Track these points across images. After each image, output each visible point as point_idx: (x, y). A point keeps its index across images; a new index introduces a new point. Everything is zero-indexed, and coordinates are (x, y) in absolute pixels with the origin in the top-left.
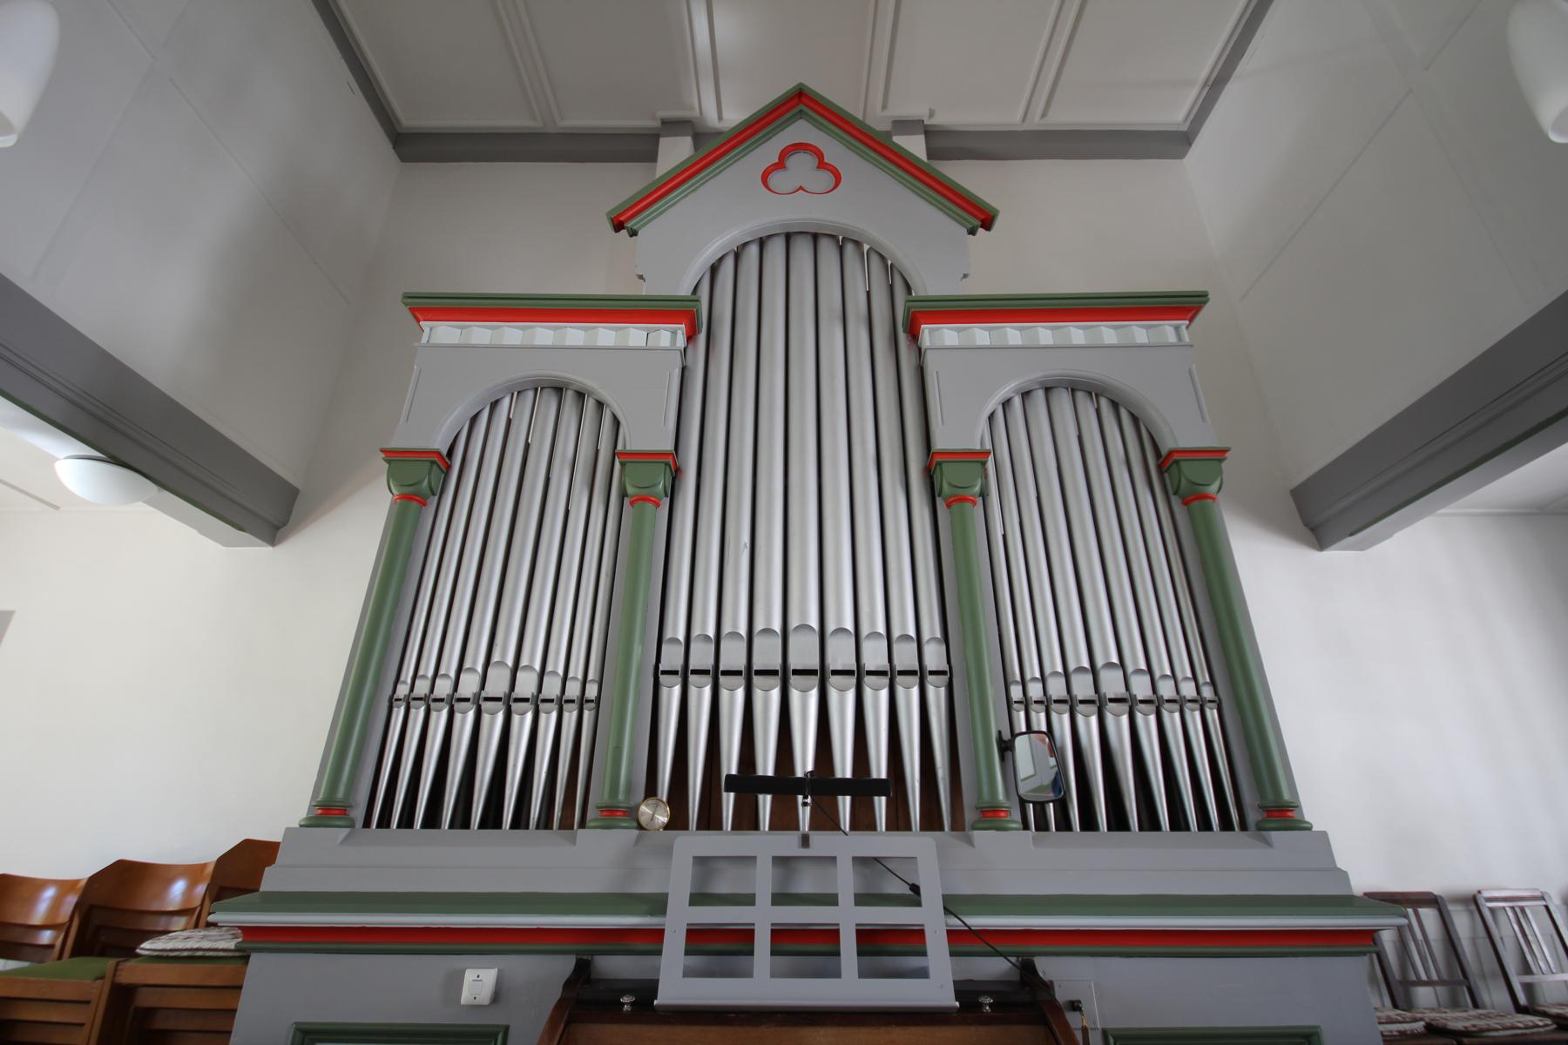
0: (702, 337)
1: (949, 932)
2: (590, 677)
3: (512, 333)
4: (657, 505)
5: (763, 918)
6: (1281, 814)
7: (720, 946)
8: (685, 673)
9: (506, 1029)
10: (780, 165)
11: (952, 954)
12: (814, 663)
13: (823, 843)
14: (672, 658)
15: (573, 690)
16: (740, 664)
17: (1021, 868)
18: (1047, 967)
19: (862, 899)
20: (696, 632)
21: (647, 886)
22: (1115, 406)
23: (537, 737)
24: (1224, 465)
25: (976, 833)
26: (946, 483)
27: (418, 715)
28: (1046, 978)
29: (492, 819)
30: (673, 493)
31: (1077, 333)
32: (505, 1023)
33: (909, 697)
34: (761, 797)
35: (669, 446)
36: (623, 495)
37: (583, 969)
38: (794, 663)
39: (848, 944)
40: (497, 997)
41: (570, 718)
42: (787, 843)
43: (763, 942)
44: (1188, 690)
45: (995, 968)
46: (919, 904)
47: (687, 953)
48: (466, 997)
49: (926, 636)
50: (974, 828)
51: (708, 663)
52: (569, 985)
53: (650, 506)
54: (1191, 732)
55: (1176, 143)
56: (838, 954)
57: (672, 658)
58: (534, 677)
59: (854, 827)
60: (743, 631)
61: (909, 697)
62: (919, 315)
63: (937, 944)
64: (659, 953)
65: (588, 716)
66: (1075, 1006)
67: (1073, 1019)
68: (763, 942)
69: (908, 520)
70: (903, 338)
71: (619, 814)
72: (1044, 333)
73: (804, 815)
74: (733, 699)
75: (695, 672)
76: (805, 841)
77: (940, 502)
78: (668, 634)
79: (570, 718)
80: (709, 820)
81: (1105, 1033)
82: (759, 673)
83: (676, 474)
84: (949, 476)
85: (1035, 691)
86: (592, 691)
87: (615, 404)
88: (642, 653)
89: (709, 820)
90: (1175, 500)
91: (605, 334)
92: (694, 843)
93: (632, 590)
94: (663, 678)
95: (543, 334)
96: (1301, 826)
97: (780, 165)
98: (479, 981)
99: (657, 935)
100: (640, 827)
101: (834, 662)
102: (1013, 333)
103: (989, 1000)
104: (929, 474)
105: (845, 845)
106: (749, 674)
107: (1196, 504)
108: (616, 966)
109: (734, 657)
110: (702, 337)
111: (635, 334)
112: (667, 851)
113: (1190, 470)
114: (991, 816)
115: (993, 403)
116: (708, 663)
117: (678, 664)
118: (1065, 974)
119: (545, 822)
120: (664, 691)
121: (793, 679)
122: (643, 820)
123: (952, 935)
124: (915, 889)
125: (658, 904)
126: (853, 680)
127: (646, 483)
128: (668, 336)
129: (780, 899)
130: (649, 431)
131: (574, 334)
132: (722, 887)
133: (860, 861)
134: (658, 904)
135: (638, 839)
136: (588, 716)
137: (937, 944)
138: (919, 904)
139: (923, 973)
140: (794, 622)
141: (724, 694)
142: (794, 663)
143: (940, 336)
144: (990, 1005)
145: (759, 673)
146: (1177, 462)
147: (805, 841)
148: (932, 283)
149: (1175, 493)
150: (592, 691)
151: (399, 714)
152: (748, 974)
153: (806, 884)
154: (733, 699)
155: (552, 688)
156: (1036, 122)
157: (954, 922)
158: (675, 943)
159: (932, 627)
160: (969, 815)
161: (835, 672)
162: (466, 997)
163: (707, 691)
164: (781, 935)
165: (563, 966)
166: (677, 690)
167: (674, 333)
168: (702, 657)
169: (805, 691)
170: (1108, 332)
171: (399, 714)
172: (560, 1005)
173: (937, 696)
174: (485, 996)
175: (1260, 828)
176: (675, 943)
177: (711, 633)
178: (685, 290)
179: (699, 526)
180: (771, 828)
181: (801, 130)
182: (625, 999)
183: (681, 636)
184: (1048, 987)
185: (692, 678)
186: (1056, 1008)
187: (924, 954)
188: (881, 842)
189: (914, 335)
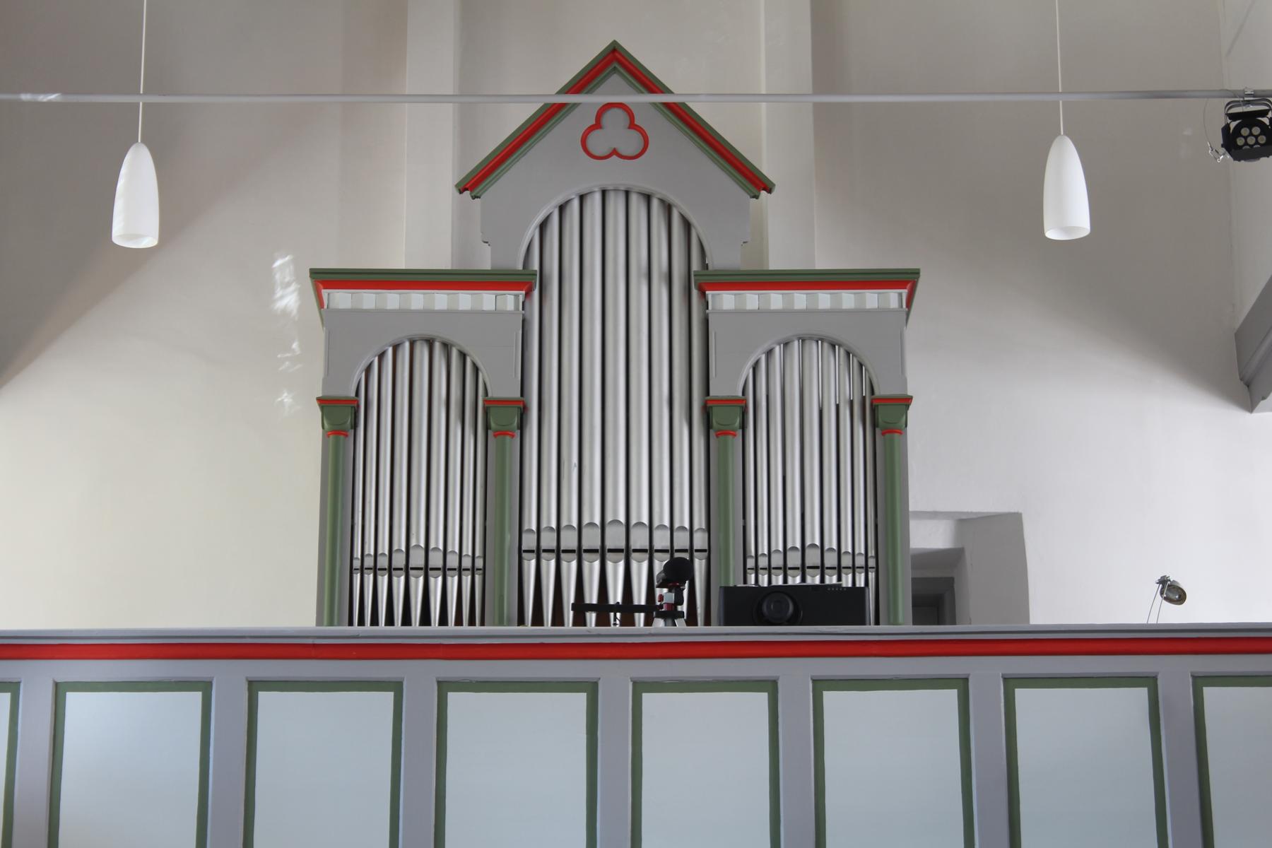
0: (536, 293)
2: (477, 554)
4: (513, 436)
10: (598, 125)
12: (622, 545)
14: (529, 542)
15: (467, 563)
16: (574, 545)
20: (544, 525)
27: (369, 578)
30: (522, 426)
34: (588, 614)
35: (517, 394)
36: (487, 427)
38: (609, 545)
41: (467, 580)
49: (696, 527)
51: (553, 545)
53: (508, 438)
57: (529, 542)
58: (441, 555)
60: (575, 524)
62: (704, 281)
65: (478, 578)
69: (688, 445)
70: (695, 293)
75: (545, 551)
77: (712, 433)
78: (526, 527)
79: (467, 580)
82: (587, 551)
84: (718, 417)
85: (763, 562)
86: (479, 563)
88: (511, 538)
94: (524, 555)
95: (417, 299)
97: (598, 125)
101: (635, 544)
109: (569, 541)
110: (536, 293)
111: (488, 300)
116: (553, 545)
117: (533, 546)
120: (525, 563)
121: (608, 555)
126: (647, 555)
127: (503, 422)
136: (478, 578)
140: (609, 518)
141: (564, 564)
142: (609, 545)
145: (587, 551)
150: (479, 563)
151: (357, 577)
155: (453, 561)
159: (700, 522)
161: (635, 551)
163: (553, 563)
166: (533, 562)
167: (516, 296)
168: (548, 541)
169: (616, 562)
170: (848, 299)
171: (357, 577)
177: (554, 525)
179: (541, 447)
181: (615, 90)
183: (534, 527)
185: (544, 555)
189: (703, 295)
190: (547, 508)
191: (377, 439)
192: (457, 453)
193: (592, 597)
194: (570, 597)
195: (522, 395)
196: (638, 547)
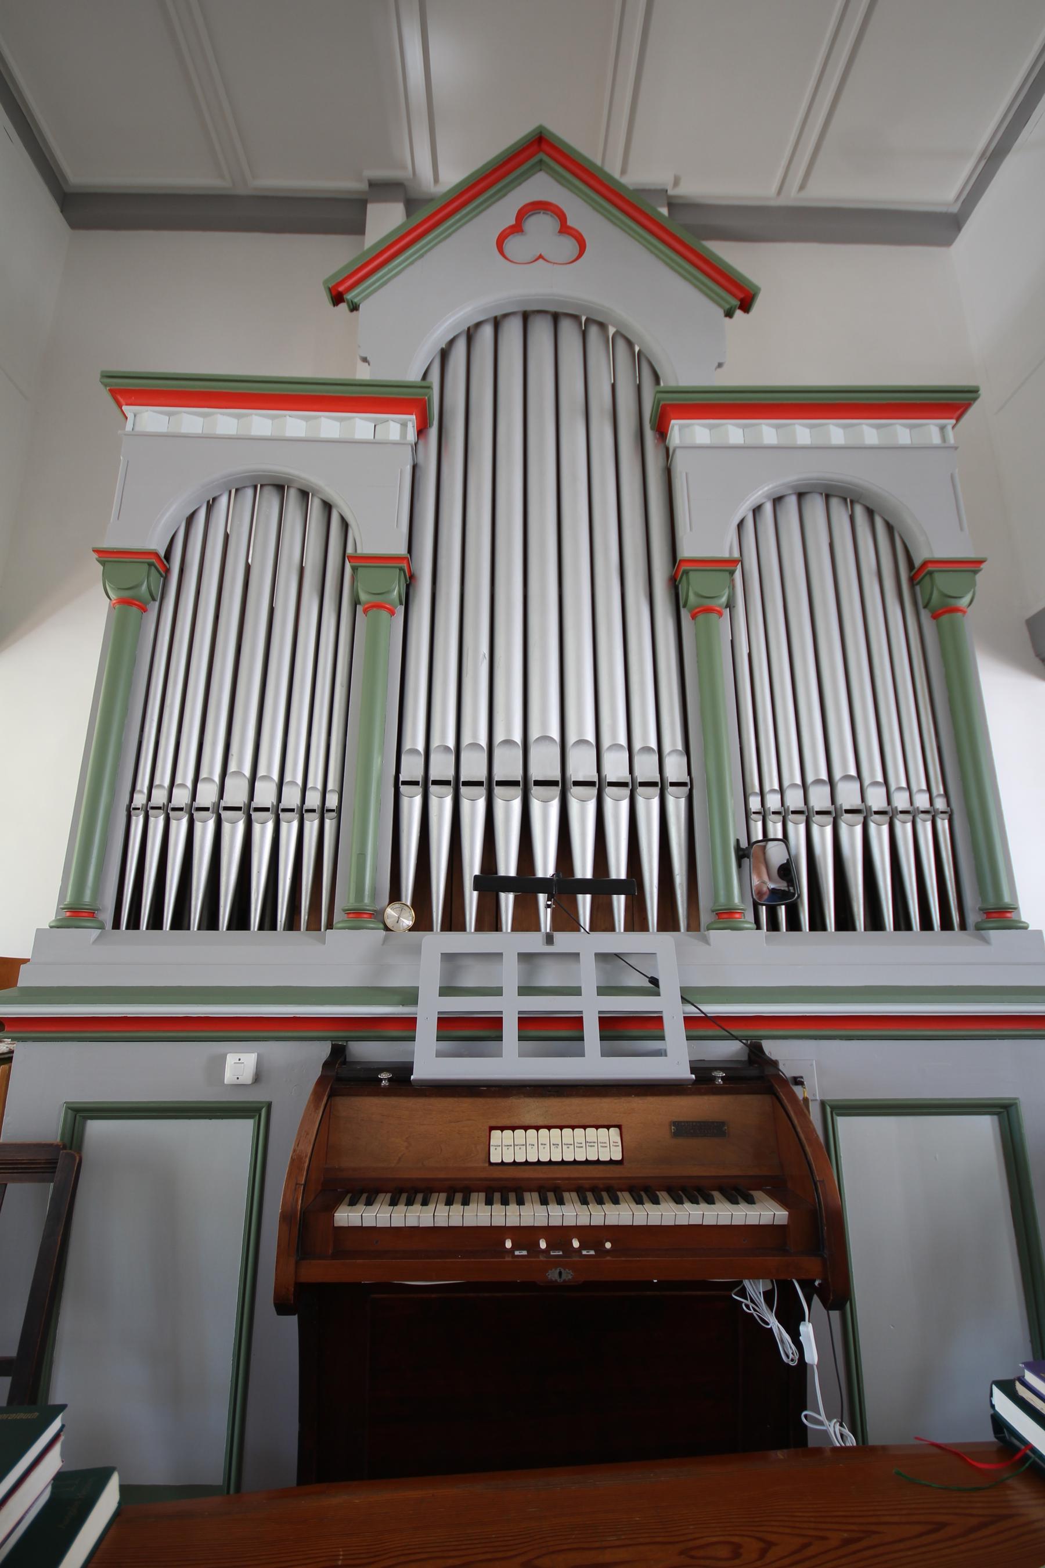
0: (433, 432)
1: (687, 1019)
2: (330, 786)
3: (226, 422)
4: (392, 613)
5: (510, 1007)
6: (1000, 915)
7: (472, 1030)
8: (426, 784)
9: (269, 1105)
10: (517, 228)
11: (689, 1038)
13: (565, 941)
14: (412, 768)
15: (313, 800)
16: (482, 775)
17: (754, 964)
18: (772, 1048)
19: (603, 991)
20: (435, 743)
21: (398, 980)
22: (870, 513)
23: (278, 846)
24: (978, 577)
25: (712, 933)
26: (690, 590)
27: (157, 824)
28: (773, 1058)
29: (240, 920)
30: (407, 602)
31: (836, 431)
32: (268, 1100)
33: (649, 807)
35: (403, 550)
36: (356, 602)
37: (338, 1053)
38: (535, 774)
39: (591, 1029)
40: (257, 1078)
42: (532, 942)
43: (510, 1029)
44: (922, 801)
45: (726, 1049)
46: (658, 994)
47: (439, 1039)
48: (229, 1077)
49: (667, 748)
50: (708, 929)
51: (449, 774)
52: (327, 1065)
53: (384, 614)
54: (920, 842)
55: (940, 227)
56: (582, 1039)
58: (273, 788)
59: (593, 928)
60: (483, 741)
61: (649, 807)
63: (674, 1028)
64: (413, 1039)
65: (329, 825)
66: (798, 1081)
67: (797, 1090)
68: (510, 1029)
69: (651, 631)
70: (649, 435)
71: (363, 916)
72: (802, 431)
73: (546, 916)
74: (474, 810)
75: (436, 783)
76: (549, 940)
77: (685, 614)
78: (407, 745)
80: (453, 921)
81: (823, 1104)
82: (500, 783)
83: (410, 582)
84: (696, 586)
86: (332, 801)
87: (344, 505)
89: (453, 921)
90: (925, 615)
91: (329, 425)
92: (438, 942)
93: (369, 699)
94: (403, 789)
95: (261, 423)
96: (1018, 926)
97: (517, 228)
98: (239, 1064)
99: (411, 1022)
100: (387, 929)
102: (768, 431)
103: (722, 1074)
104: (674, 584)
105: (586, 943)
106: (490, 785)
107: (945, 618)
108: (368, 1051)
109: (474, 767)
110: (433, 432)
111: (361, 425)
112: (416, 950)
113: (943, 582)
114: (726, 917)
115: (744, 510)
116: (449, 774)
117: (418, 775)
118: (787, 1054)
119: (292, 924)
120: (405, 801)
121: (535, 790)
122: (389, 923)
123: (689, 1021)
124: (654, 981)
125: (410, 996)
126: (593, 791)
127: (378, 589)
128: (397, 428)
129: (525, 991)
130: (379, 533)
131: (294, 424)
132: (469, 981)
133: (602, 957)
134: (410, 996)
135: (385, 940)
136: (329, 825)
137: (674, 1028)
138: (658, 994)
139: (661, 1053)
140: (534, 734)
141: (465, 805)
142: (535, 774)
143: (690, 433)
144: (722, 1078)
145: (500, 783)
146: (931, 573)
147: (549, 940)
148: (684, 372)
149: (925, 607)
150: (332, 801)
152: (499, 1055)
153: (550, 976)
154: (474, 810)
155: (291, 797)
156: (792, 197)
157: (691, 1010)
158: (427, 1029)
159: (673, 739)
160: (705, 917)
161: (577, 783)
162: (229, 1077)
163: (448, 802)
164: (526, 1022)
165: (322, 1050)
166: (418, 801)
167: (404, 425)
168: (442, 767)
169: (546, 801)
170: (869, 431)
172: (321, 1082)
173: (676, 807)
174: (247, 1075)
175: (979, 928)
176: (427, 1029)
177: (451, 743)
178: (414, 376)
179: (436, 635)
180: (513, 930)
181: (540, 186)
182: (383, 1076)
183: (420, 747)
184: (774, 1064)
185: (433, 789)
186: (784, 1081)
187: (662, 1038)
188: (620, 940)
189: (662, 432)
190: (442, 723)
191: (192, 615)
192: (309, 636)
193: (508, 866)
194: (473, 865)
195: (410, 550)
196: (674, 780)
